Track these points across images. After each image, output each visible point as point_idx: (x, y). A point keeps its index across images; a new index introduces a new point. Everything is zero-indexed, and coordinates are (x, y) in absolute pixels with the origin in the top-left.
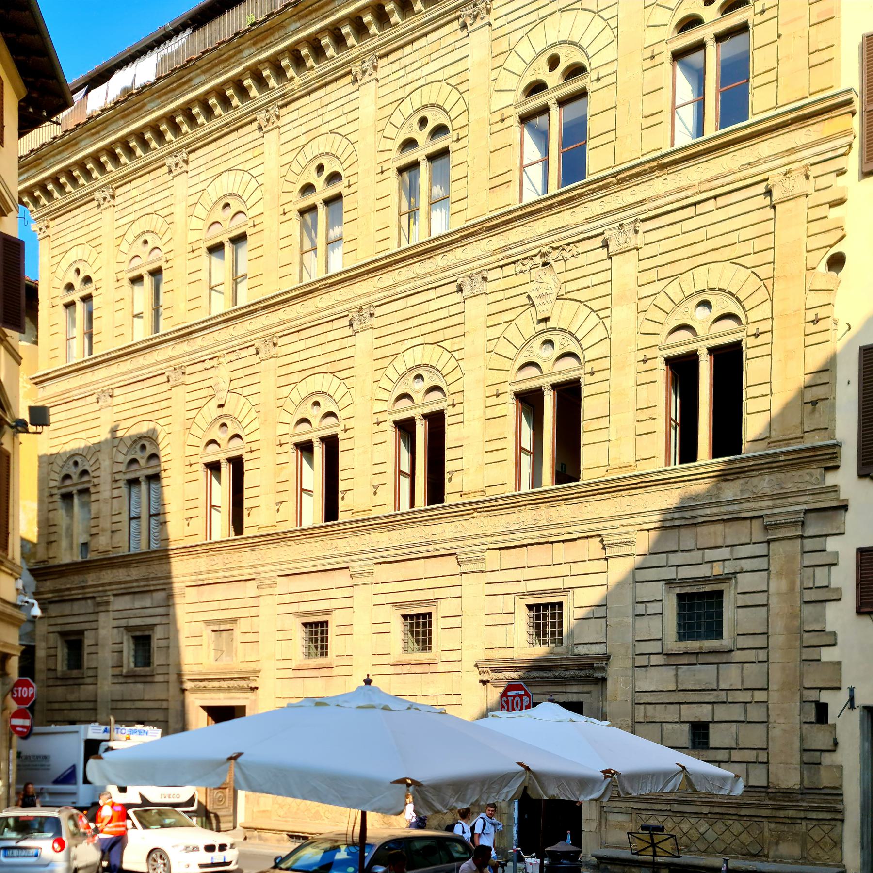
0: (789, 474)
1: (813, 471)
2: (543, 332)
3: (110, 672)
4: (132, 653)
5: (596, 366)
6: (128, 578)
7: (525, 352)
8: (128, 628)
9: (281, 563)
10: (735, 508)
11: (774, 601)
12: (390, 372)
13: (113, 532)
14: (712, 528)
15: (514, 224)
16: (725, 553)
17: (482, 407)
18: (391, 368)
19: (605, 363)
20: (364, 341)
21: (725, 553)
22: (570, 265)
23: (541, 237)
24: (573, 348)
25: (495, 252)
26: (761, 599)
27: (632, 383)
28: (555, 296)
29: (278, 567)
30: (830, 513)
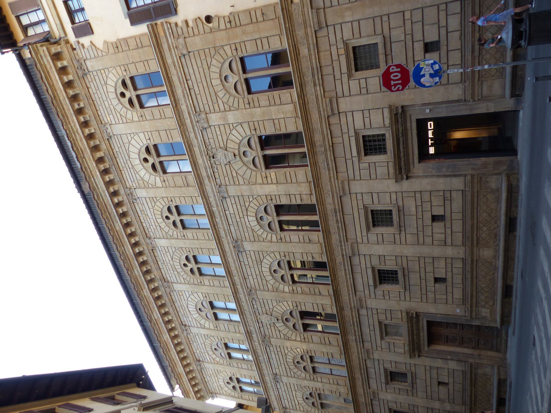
2: (240, 157)
3: (411, 397)
4: (400, 383)
5: (252, 128)
6: (360, 379)
7: (249, 165)
8: (387, 383)
9: (349, 294)
10: (312, 46)
11: (357, 17)
12: (260, 233)
13: (338, 384)
14: (322, 58)
15: (199, 173)
16: (334, 49)
17: (272, 185)
18: (258, 232)
19: (251, 124)
20: (247, 246)
21: (334, 49)
22: (214, 146)
23: (203, 160)
24: (246, 141)
25: (210, 182)
26: (356, 24)
27: (259, 109)
28: (226, 152)
29: (351, 296)
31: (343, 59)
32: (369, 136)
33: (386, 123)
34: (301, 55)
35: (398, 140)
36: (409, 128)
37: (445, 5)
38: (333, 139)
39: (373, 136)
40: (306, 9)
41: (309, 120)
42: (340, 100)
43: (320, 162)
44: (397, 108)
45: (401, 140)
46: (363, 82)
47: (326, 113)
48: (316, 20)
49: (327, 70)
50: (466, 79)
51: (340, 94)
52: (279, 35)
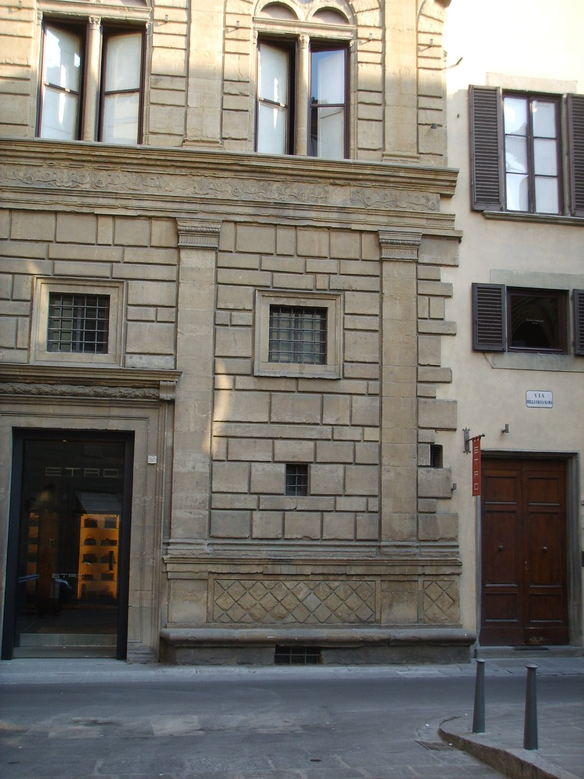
0: (405, 193)
1: (429, 195)
11: (387, 326)
30: (445, 243)
31: (306, 282)
32: (106, 312)
33: (136, 358)
34: (331, 188)
35: (87, 382)
36: (115, 411)
37: (376, 509)
38: (110, 221)
39: (105, 325)
40: (423, 222)
41: (171, 171)
42: (210, 257)
43: (50, 171)
44: (173, 388)
45: (87, 390)
46: (247, 318)
47: (183, 215)
48: (400, 238)
49: (285, 239)
50: (216, 547)
51: (224, 260)
52: (384, 149)
